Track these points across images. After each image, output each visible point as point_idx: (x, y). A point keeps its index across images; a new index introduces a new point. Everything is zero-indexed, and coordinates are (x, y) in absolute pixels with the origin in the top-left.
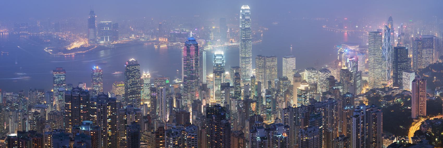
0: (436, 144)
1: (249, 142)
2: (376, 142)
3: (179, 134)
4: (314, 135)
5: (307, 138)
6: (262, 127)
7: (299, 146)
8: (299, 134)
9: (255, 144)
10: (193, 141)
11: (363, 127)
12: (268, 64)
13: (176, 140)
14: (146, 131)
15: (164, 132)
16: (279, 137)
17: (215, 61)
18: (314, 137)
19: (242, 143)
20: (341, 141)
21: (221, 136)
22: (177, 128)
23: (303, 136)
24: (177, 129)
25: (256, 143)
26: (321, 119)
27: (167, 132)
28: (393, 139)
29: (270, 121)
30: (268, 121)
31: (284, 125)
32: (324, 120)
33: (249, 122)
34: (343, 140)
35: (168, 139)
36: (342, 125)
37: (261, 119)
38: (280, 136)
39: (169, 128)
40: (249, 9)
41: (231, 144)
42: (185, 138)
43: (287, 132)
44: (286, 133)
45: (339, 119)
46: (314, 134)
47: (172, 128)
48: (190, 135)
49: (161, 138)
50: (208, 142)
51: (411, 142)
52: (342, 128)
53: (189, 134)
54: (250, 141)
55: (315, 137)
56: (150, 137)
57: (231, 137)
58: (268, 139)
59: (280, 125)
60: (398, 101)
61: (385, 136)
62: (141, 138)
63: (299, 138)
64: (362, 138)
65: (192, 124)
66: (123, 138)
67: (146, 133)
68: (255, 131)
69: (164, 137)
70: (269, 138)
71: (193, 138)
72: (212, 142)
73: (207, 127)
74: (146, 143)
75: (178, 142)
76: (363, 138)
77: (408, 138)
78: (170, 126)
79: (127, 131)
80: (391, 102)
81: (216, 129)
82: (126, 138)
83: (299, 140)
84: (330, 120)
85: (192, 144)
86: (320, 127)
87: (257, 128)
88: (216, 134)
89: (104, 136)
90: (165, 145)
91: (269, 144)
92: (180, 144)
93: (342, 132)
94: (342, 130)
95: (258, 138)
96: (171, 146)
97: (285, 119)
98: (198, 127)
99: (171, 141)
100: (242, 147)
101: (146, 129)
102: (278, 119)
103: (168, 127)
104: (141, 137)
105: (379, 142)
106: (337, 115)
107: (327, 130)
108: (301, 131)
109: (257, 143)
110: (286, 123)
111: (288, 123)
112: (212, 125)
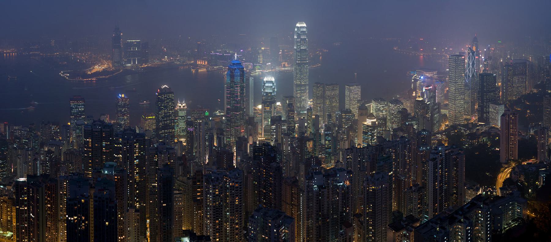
1: (304, 191)
2: (456, 194)
3: (221, 180)
4: (382, 184)
5: (374, 187)
6: (320, 173)
7: (364, 197)
8: (365, 182)
9: (312, 194)
10: (237, 190)
11: (441, 174)
12: (328, 93)
13: (217, 189)
14: (181, 175)
15: (202, 178)
16: (340, 185)
17: (264, 90)
18: (382, 186)
19: (296, 193)
20: (414, 191)
21: (271, 183)
22: (218, 172)
23: (369, 185)
24: (218, 174)
25: (313, 194)
26: (391, 163)
27: (206, 177)
28: (478, 190)
29: (329, 165)
30: (327, 165)
31: (346, 169)
32: (395, 164)
33: (304, 165)
34: (417, 190)
35: (207, 187)
36: (417, 171)
37: (319, 162)
38: (342, 184)
39: (208, 172)
40: (306, 26)
41: (283, 194)
42: (228, 186)
43: (350, 179)
44: (349, 181)
45: (412, 164)
46: (382, 182)
47: (212, 172)
48: (233, 182)
49: (199, 186)
50: (255, 191)
51: (499, 193)
52: (416, 175)
53: (233, 180)
54: (305, 191)
55: (384, 186)
56: (186, 184)
57: (283, 185)
58: (327, 188)
59: (341, 170)
61: (468, 185)
62: (175, 185)
63: (364, 188)
64: (440, 188)
65: (235, 167)
66: (153, 184)
67: (181, 178)
68: (312, 178)
69: (202, 184)
70: (328, 187)
71: (237, 185)
72: (259, 192)
73: (254, 171)
74: (181, 192)
75: (219, 191)
76: (441, 187)
77: (495, 189)
78: (209, 170)
79: (158, 175)
81: (264, 175)
82: (156, 185)
83: (364, 190)
84: (402, 164)
85: (236, 193)
86: (390, 174)
87: (314, 174)
88: (264, 181)
89: (131, 181)
90: (203, 195)
91: (328, 195)
92: (222, 193)
93: (416, 179)
94: (416, 177)
95: (315, 186)
96: (211, 196)
97: (348, 162)
98: (243, 172)
99: (211, 189)
100: (296, 198)
101: (180, 174)
102: (339, 162)
103: (207, 171)
104: (175, 184)
105: (461, 194)
106: (411, 158)
107: (398, 177)
108: (367, 178)
109: (314, 193)
110: (348, 167)
111: (351, 167)
112: (259, 169)
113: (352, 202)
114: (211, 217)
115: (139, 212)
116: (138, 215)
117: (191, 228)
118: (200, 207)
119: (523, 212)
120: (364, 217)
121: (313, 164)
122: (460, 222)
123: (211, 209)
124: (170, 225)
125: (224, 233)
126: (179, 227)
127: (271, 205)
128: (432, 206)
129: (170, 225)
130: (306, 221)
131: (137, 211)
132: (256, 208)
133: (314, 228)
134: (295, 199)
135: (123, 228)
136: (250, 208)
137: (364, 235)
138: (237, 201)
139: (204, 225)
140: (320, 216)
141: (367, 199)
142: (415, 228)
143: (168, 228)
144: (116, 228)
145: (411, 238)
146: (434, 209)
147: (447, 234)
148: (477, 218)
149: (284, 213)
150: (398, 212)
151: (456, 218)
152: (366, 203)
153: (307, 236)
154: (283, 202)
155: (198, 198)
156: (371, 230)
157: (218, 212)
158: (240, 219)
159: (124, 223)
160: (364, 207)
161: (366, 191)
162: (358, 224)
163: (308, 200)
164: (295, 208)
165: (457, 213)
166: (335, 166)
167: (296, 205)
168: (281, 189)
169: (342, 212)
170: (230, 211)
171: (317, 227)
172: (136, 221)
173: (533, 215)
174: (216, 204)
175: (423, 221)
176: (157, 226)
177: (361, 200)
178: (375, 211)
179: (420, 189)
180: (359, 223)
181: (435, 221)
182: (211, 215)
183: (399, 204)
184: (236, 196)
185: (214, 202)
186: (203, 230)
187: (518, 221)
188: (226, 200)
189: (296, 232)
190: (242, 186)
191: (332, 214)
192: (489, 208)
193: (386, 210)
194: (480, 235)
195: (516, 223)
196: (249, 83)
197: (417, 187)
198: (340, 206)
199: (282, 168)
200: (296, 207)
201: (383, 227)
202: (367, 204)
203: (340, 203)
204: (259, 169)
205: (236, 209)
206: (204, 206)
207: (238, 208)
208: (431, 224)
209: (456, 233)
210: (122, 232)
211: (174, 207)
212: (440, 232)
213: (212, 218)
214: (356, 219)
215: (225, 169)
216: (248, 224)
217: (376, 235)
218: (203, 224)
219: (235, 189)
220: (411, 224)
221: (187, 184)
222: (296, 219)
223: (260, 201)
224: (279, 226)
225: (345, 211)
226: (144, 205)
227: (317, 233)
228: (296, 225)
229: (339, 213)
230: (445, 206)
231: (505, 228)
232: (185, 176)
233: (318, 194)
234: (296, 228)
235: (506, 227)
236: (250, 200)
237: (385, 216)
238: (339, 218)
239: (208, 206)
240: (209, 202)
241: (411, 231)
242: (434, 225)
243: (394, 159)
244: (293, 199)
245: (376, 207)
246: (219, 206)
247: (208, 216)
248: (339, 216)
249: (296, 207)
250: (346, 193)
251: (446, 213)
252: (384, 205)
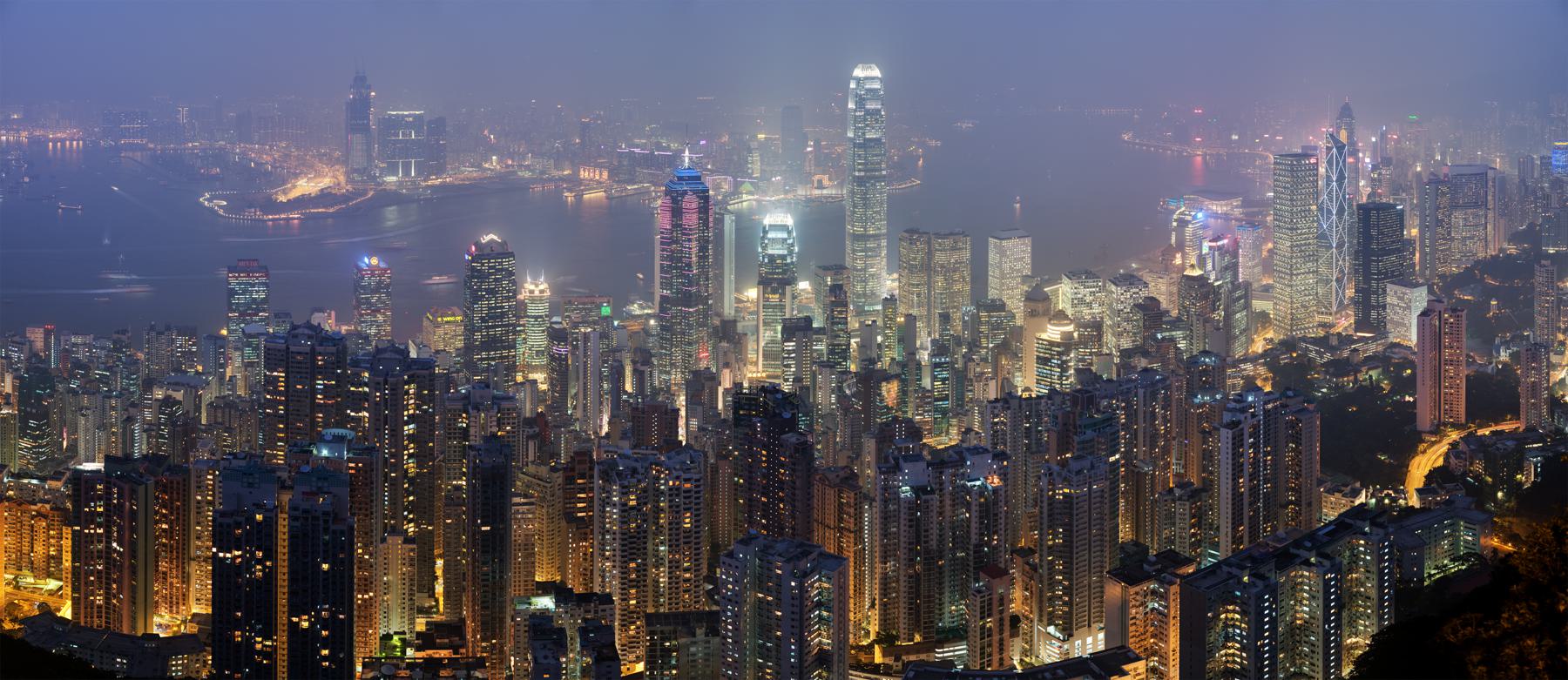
0: (1500, 508)
1: (874, 500)
2: (1295, 503)
5: (1067, 491)
6: (918, 457)
7: (1041, 513)
8: (1043, 478)
9: (895, 507)
10: (689, 497)
11: (1254, 458)
12: (940, 257)
13: (632, 493)
14: (533, 462)
15: (591, 469)
17: (764, 248)
18: (1090, 488)
20: (1180, 499)
21: (781, 482)
23: (1054, 485)
24: (636, 460)
25: (899, 506)
26: (1114, 433)
27: (601, 467)
28: (1356, 493)
29: (944, 438)
32: (1125, 435)
35: (604, 489)
37: (915, 432)
38: (978, 483)
42: (662, 487)
44: (999, 475)
47: (619, 455)
48: (678, 478)
50: (736, 500)
51: (1414, 501)
53: (675, 474)
54: (877, 499)
58: (937, 492)
59: (977, 451)
60: (1371, 376)
61: (1329, 485)
62: (515, 485)
63: (1042, 491)
64: (1250, 490)
65: (684, 443)
67: (531, 469)
68: (897, 468)
70: (941, 490)
71: (688, 486)
72: (750, 500)
74: (532, 500)
75: (637, 499)
76: (1254, 491)
77: (1403, 492)
78: (610, 449)
80: (1348, 382)
81: (765, 462)
82: (464, 483)
83: (1042, 496)
85: (685, 504)
86: (1112, 459)
87: (901, 461)
88: (764, 476)
90: (593, 506)
91: (941, 508)
92: (645, 504)
94: (1185, 467)
100: (852, 514)
101: (531, 458)
102: (973, 433)
103: (605, 452)
105: (1309, 504)
106: (1169, 421)
107: (1136, 467)
108: (1050, 469)
109: (902, 503)
110: (997, 444)
111: (1005, 445)
112: (750, 448)
113: (1006, 524)
114: (614, 556)
115: (414, 543)
116: (413, 550)
117: (559, 578)
118: (586, 534)
119: (1482, 541)
120: (1041, 556)
121: (900, 435)
122: (1307, 563)
123: (614, 539)
124: (501, 572)
125: (650, 588)
126: (526, 576)
127: (783, 529)
128: (1230, 530)
129: (501, 572)
130: (878, 566)
131: (408, 540)
132: (741, 536)
133: (902, 578)
134: (850, 517)
135: (371, 577)
136: (723, 537)
137: (1041, 591)
138: (687, 520)
139: (596, 574)
140: (918, 554)
141: (1049, 516)
142: (1182, 577)
143: (494, 578)
144: (352, 577)
145: (1172, 597)
146: (1233, 537)
147: (1273, 590)
148: (1355, 557)
149: (820, 547)
150: (1136, 543)
151: (1298, 556)
152: (1045, 526)
153: (880, 594)
154: (815, 524)
155: (579, 515)
156: (1060, 582)
157: (633, 546)
158: (696, 560)
159: (372, 566)
160: (1041, 535)
161: (1045, 499)
162: (1024, 570)
163: (886, 519)
165: (1298, 544)
166: (962, 441)
168: (809, 494)
169: (980, 545)
170: (667, 544)
171: (910, 577)
172: (407, 561)
173: (1509, 547)
174: (629, 529)
175: (1203, 562)
176: (464, 574)
178: (1072, 504)
179: (1197, 494)
180: (1027, 567)
181: (1238, 560)
182: (614, 550)
183: (1137, 527)
184: (685, 509)
185: (624, 521)
186: (592, 583)
187: (1468, 561)
188: (658, 518)
189: (852, 587)
190: (702, 488)
191: (953, 550)
192: (1387, 535)
193: (1102, 540)
194: (1362, 590)
195: (1463, 564)
198: (974, 531)
199: (812, 446)
202: (1050, 527)
203: (974, 525)
204: (750, 448)
206: (596, 531)
208: (1225, 569)
209: (1295, 587)
210: (366, 585)
212: (1251, 584)
213: (618, 558)
214: (1018, 560)
215: (656, 449)
216: (718, 570)
217: (1075, 592)
218: (592, 571)
219: (683, 494)
220: (1169, 570)
222: (852, 559)
223: (751, 523)
224: (806, 574)
225: (988, 544)
227: (911, 587)
228: (851, 573)
229: (971, 547)
230: (1265, 531)
231: (1430, 576)
233: (912, 506)
234: (852, 578)
235: (1435, 574)
236: (723, 520)
237: (1099, 543)
238: (971, 558)
240: (610, 523)
241: (1171, 583)
242: (1235, 571)
243: (1123, 424)
244: (842, 518)
245: (1075, 534)
246: (639, 533)
247: (607, 553)
248: (972, 553)
249: (852, 535)
250: (990, 507)
251: (1268, 545)
252: (1097, 530)
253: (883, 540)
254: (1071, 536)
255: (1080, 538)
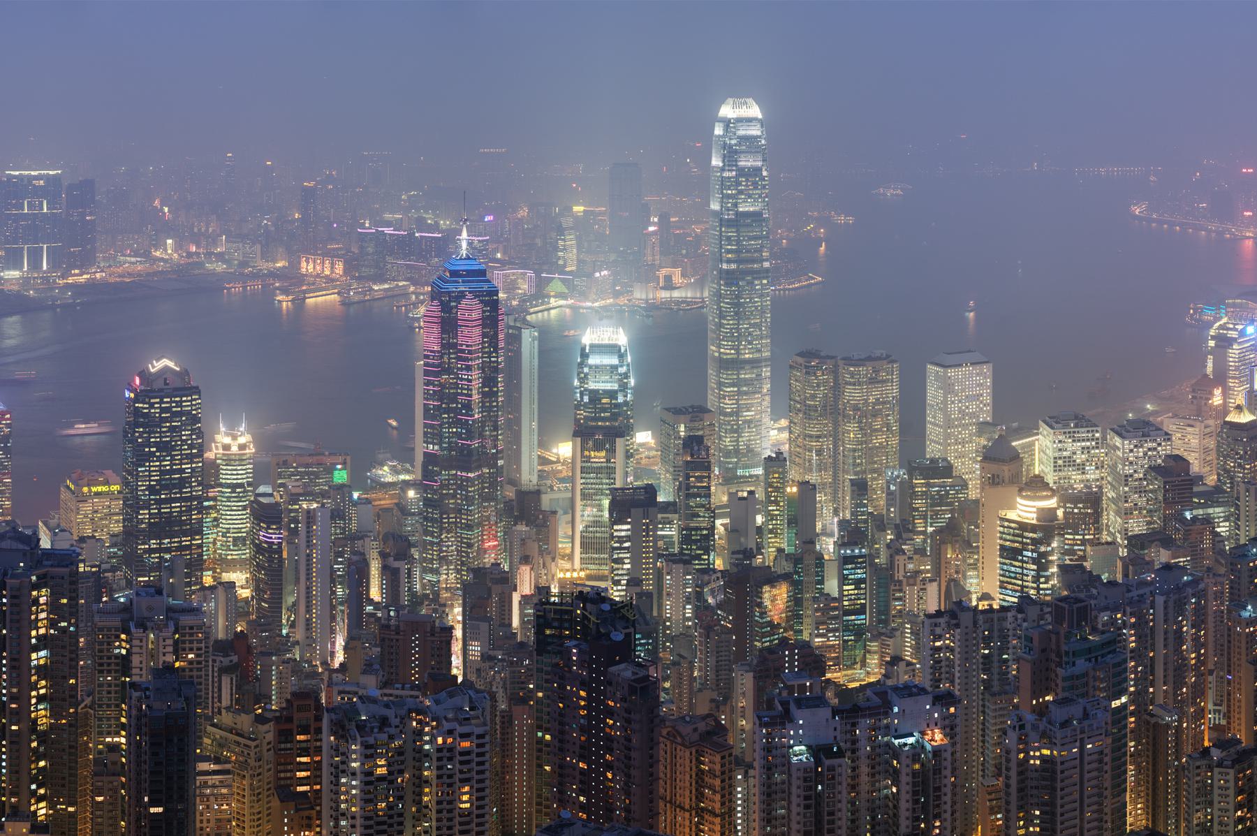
1: (750, 766)
3: (397, 727)
4: (1082, 740)
5: (1046, 752)
6: (818, 701)
7: (1008, 786)
8: (1010, 732)
10: (468, 762)
13: (381, 756)
14: (228, 709)
15: (318, 719)
16: (905, 745)
17: (583, 380)
18: (1082, 748)
19: (718, 773)
20: (1220, 765)
21: (609, 739)
22: (385, 699)
23: (1026, 743)
24: (387, 706)
25: (790, 775)
26: (1119, 664)
27: (333, 716)
29: (858, 672)
30: (850, 672)
31: (929, 689)
32: (1135, 667)
33: (752, 674)
34: (1233, 761)
35: (337, 750)
36: (1229, 694)
37: (814, 662)
38: (911, 740)
39: (343, 699)
40: (760, 116)
41: (662, 775)
42: (427, 747)
43: (947, 722)
44: (943, 728)
45: (1211, 666)
46: (1082, 732)
47: (360, 698)
48: (450, 732)
49: (304, 745)
50: (540, 766)
52: (1229, 706)
53: (447, 726)
54: (756, 764)
55: (1090, 746)
56: (250, 739)
57: (662, 745)
58: (848, 754)
59: (909, 691)
62: (201, 744)
63: (1008, 752)
65: (460, 679)
66: (108, 740)
67: (226, 718)
68: (785, 718)
69: (316, 740)
70: (853, 751)
71: (466, 744)
72: (561, 767)
73: (540, 694)
74: (228, 766)
75: (389, 765)
78: (347, 689)
79: (130, 707)
81: (583, 708)
82: (123, 740)
83: (1008, 760)
84: (1165, 670)
86: (1115, 704)
87: (793, 707)
88: (583, 730)
89: (14, 728)
90: (320, 776)
91: (853, 778)
92: (401, 772)
93: (1229, 723)
94: (1228, 716)
95: (796, 748)
96: (354, 783)
97: (938, 662)
98: (493, 697)
99: (354, 756)
101: (226, 701)
102: (902, 664)
103: (340, 693)
104: (201, 738)
106: (1203, 645)
107: (1152, 716)
108: (1020, 720)
109: (794, 771)
110: (939, 681)
111: (952, 682)
112: (562, 687)
113: (954, 803)
118: (309, 818)
121: (791, 667)
123: (353, 826)
127: (612, 811)
132: (547, 822)
134: (715, 792)
136: (520, 823)
138: (465, 798)
141: (1020, 790)
152: (1013, 807)
154: (661, 804)
155: (300, 789)
161: (1013, 765)
164: (713, 824)
166: (885, 676)
167: (717, 811)
168: (651, 757)
174: (376, 810)
177: (993, 796)
178: (1054, 772)
183: (1154, 808)
184: (462, 781)
185: (368, 799)
188: (421, 794)
190: (487, 747)
196: (518, 353)
197: (1232, 750)
199: (655, 684)
200: (718, 820)
201: (1086, 809)
202: (1020, 808)
203: (904, 805)
204: (562, 687)
205: (461, 824)
206: (326, 813)
207: (468, 823)
211: (198, 818)
215: (414, 687)
219: (459, 758)
221: (254, 740)
223: (563, 801)
226: (71, 809)
232: (244, 710)
233: (810, 776)
236: (520, 797)
239: (343, 814)
240: (347, 801)
243: (1132, 651)
244: (702, 794)
245: (1059, 819)
246: (391, 817)
249: (718, 820)
252: (1093, 812)
253: (764, 828)
254: (1053, 822)
255: (1067, 824)
